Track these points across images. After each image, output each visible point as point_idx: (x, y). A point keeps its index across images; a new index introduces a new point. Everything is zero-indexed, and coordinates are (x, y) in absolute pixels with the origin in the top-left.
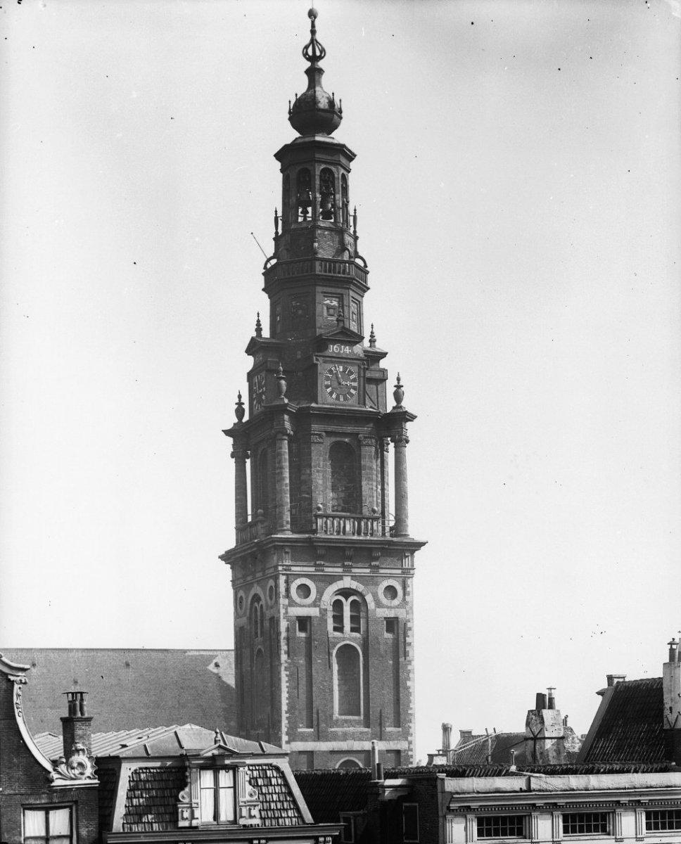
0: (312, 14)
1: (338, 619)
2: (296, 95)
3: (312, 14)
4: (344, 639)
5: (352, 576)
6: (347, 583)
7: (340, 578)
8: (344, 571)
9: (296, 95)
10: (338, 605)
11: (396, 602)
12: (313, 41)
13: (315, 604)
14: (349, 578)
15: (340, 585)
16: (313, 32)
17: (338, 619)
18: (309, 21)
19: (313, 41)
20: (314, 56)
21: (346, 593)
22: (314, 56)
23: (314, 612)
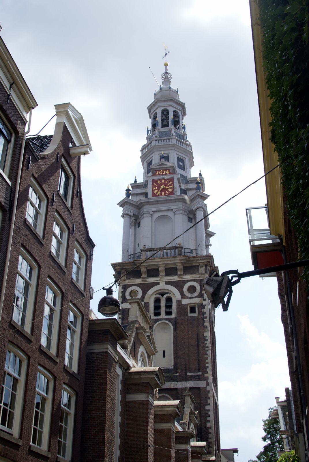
0: (166, 65)
1: (157, 308)
2: (155, 91)
3: (166, 65)
4: (160, 320)
5: (165, 282)
6: (162, 286)
7: (158, 284)
8: (160, 280)
9: (155, 91)
11: (196, 294)
12: (166, 73)
14: (165, 283)
16: (166, 70)
17: (157, 308)
18: (164, 67)
19: (166, 73)
20: (166, 78)
22: (166, 78)
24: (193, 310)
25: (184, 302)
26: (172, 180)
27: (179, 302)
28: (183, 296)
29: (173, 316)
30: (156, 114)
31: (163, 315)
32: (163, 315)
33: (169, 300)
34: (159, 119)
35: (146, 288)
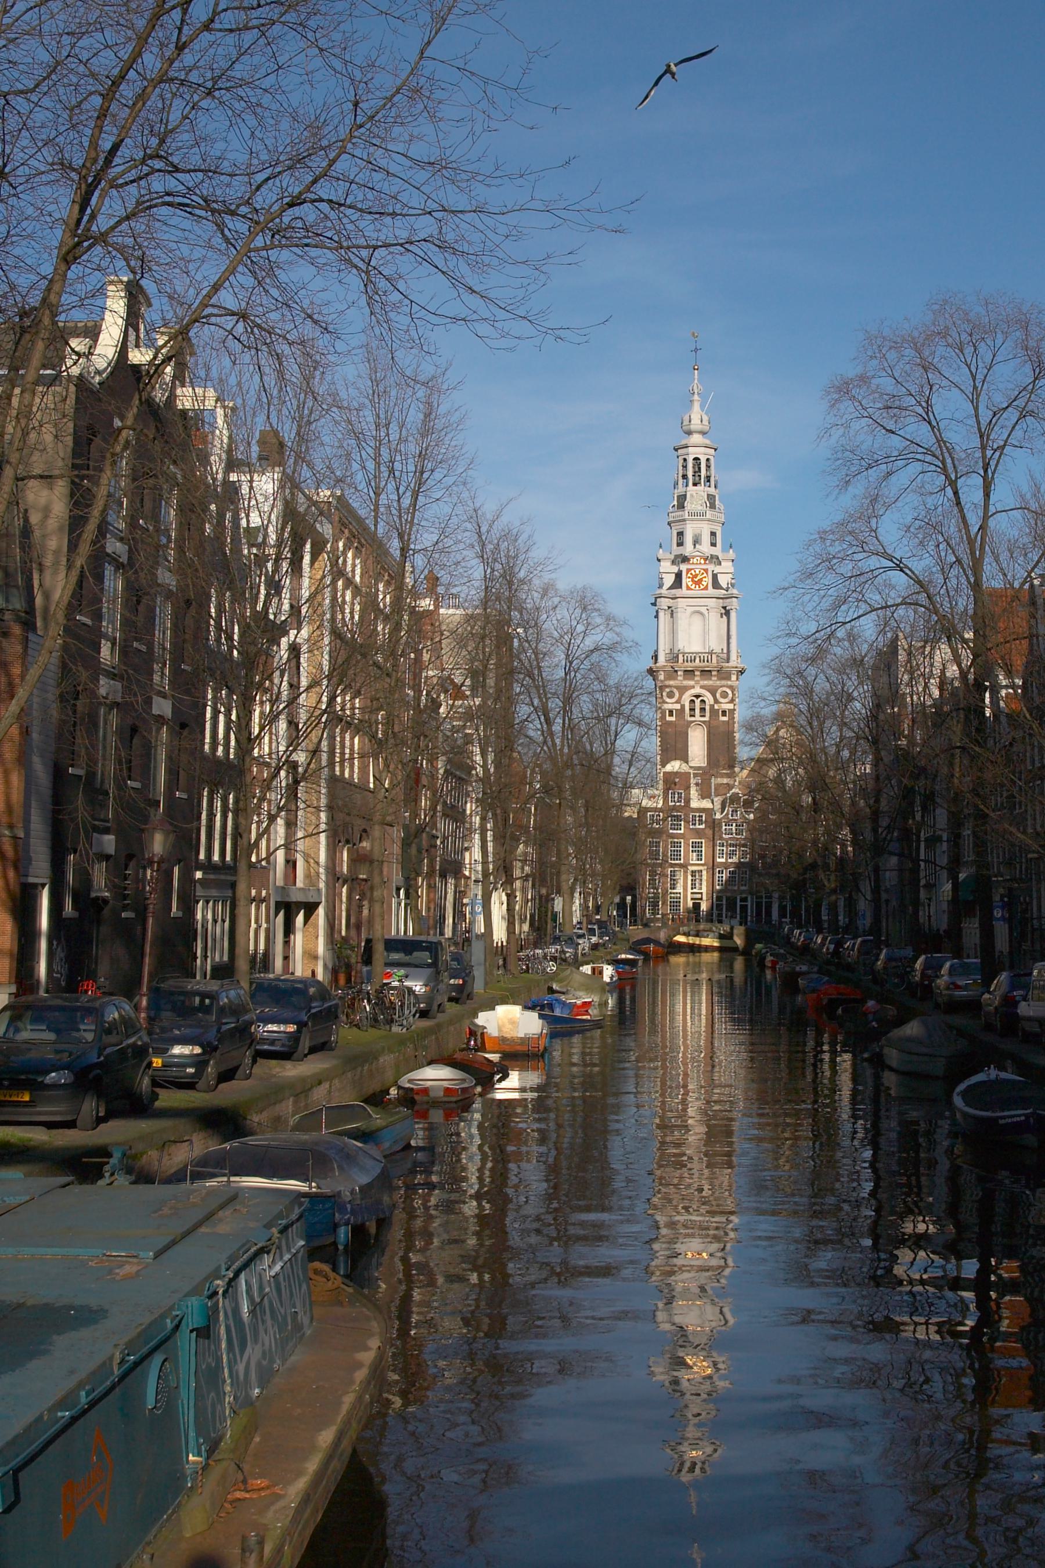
1: (692, 710)
6: (697, 690)
7: (693, 687)
10: (692, 701)
13: (676, 702)
15: (693, 692)
17: (692, 710)
21: (697, 696)
23: (678, 706)
24: (724, 713)
25: (716, 707)
26: (706, 571)
27: (712, 707)
28: (716, 701)
29: (707, 719)
30: (685, 460)
31: (698, 718)
32: (698, 718)
33: (703, 701)
34: (690, 473)
35: (683, 690)
